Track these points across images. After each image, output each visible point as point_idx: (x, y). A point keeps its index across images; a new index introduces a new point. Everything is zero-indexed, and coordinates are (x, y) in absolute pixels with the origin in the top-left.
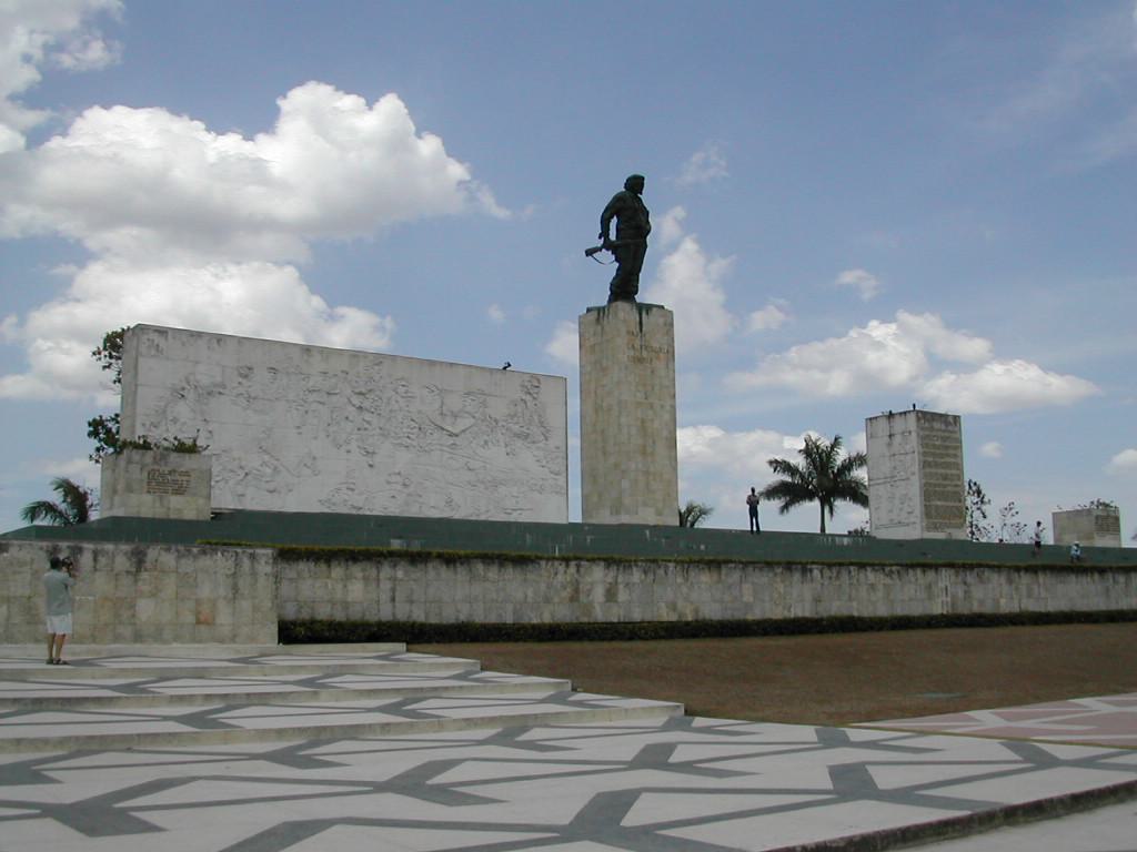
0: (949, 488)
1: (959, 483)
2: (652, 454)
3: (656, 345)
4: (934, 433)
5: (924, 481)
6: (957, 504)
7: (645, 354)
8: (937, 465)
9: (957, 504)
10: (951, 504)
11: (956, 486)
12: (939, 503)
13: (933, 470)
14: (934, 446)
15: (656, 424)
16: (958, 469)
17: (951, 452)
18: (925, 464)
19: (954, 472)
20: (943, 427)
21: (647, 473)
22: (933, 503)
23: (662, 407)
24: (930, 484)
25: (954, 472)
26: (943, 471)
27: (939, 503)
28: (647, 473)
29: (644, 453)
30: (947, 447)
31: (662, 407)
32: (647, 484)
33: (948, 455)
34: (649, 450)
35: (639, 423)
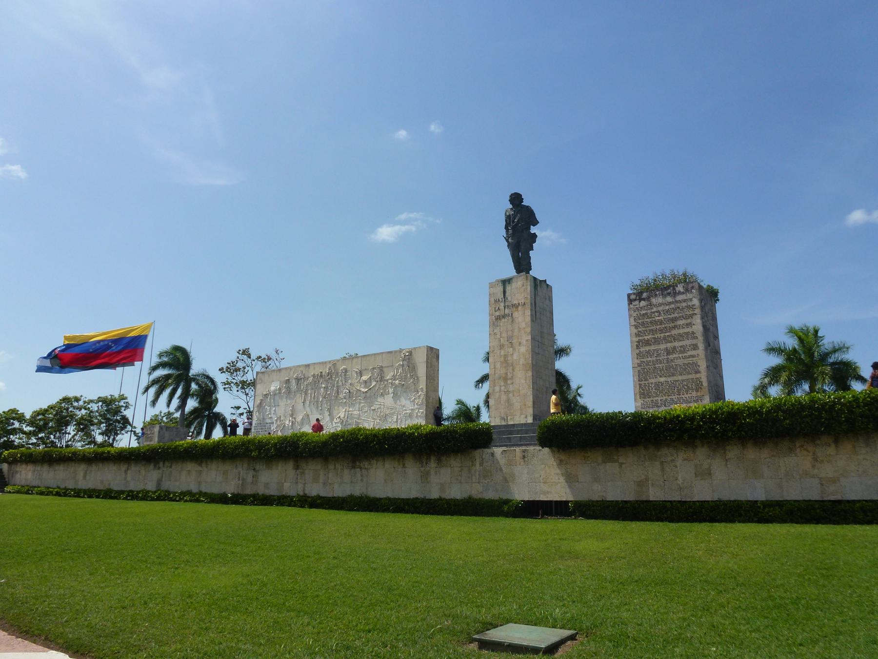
0: (679, 362)
2: (512, 378)
3: (516, 302)
4: (655, 309)
6: (693, 376)
7: (507, 311)
8: (657, 341)
9: (693, 376)
13: (653, 348)
14: (656, 323)
15: (515, 357)
21: (507, 392)
23: (520, 344)
26: (669, 345)
28: (507, 392)
29: (505, 379)
30: (676, 319)
31: (520, 344)
32: (508, 400)
33: (675, 327)
34: (509, 376)
35: (502, 359)
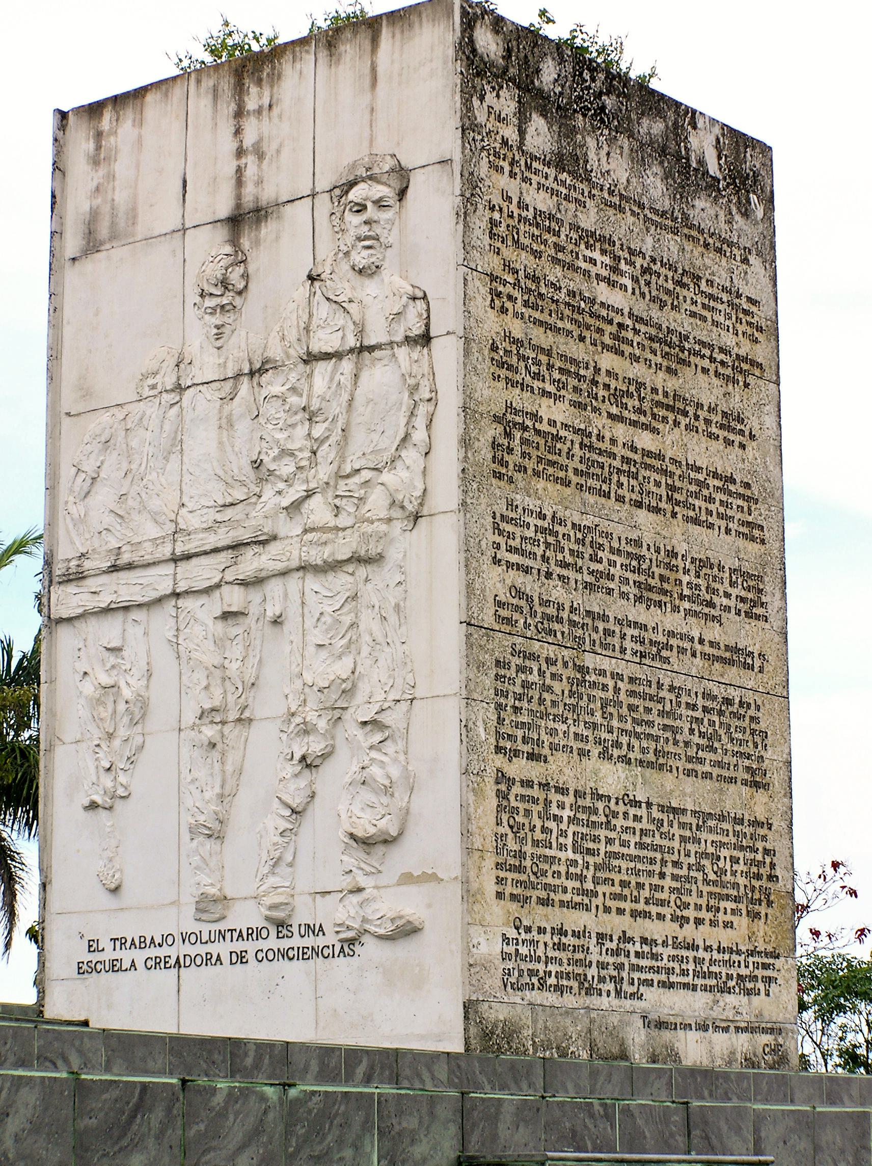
0: (686, 671)
1: (748, 635)
5: (497, 582)
6: (735, 798)
9: (735, 798)
10: (691, 794)
11: (736, 657)
12: (612, 778)
14: (585, 315)
16: (752, 531)
17: (704, 389)
18: (509, 448)
19: (722, 547)
20: (655, 187)
22: (561, 768)
24: (549, 621)
25: (722, 547)
27: (612, 778)
